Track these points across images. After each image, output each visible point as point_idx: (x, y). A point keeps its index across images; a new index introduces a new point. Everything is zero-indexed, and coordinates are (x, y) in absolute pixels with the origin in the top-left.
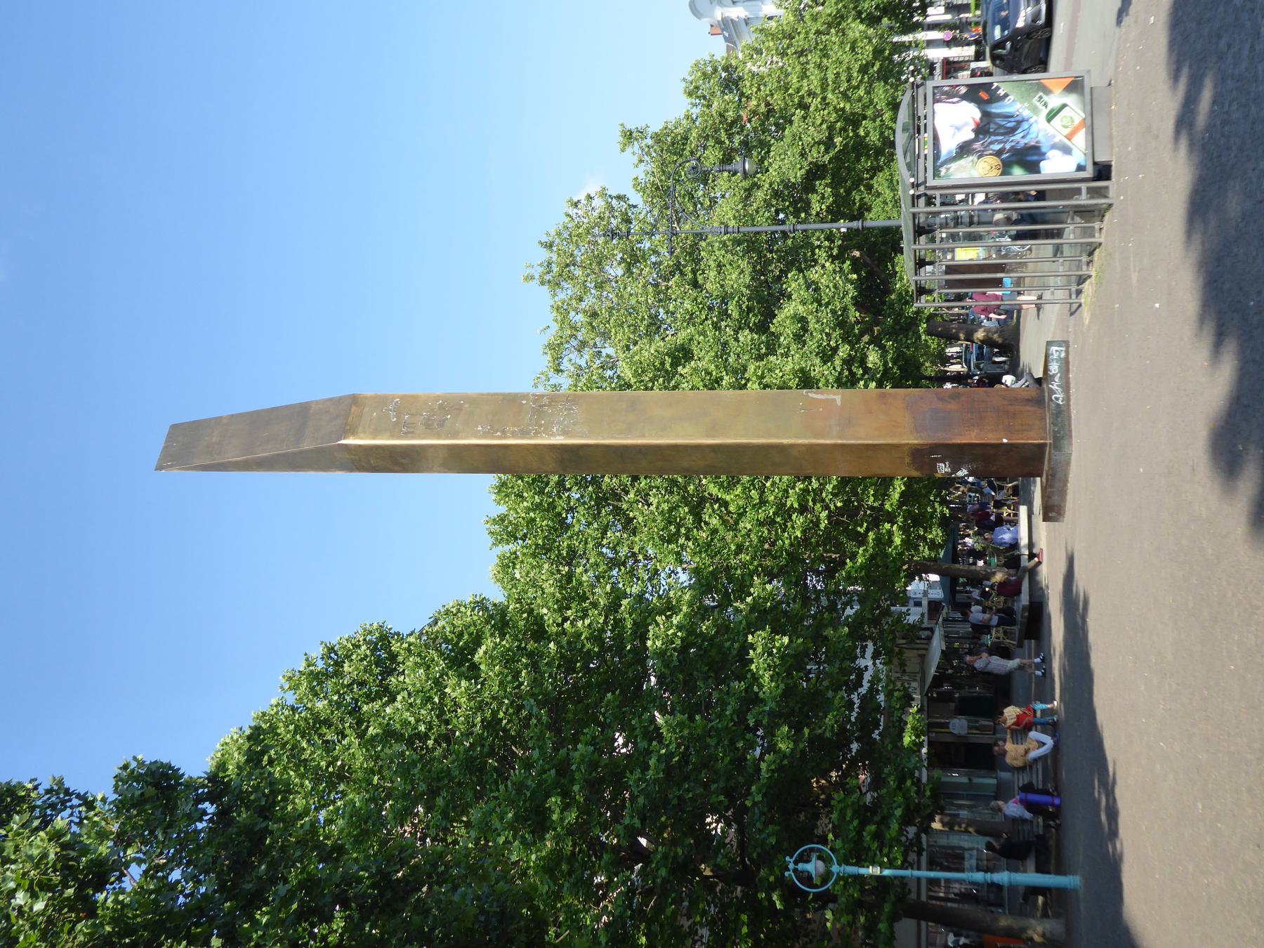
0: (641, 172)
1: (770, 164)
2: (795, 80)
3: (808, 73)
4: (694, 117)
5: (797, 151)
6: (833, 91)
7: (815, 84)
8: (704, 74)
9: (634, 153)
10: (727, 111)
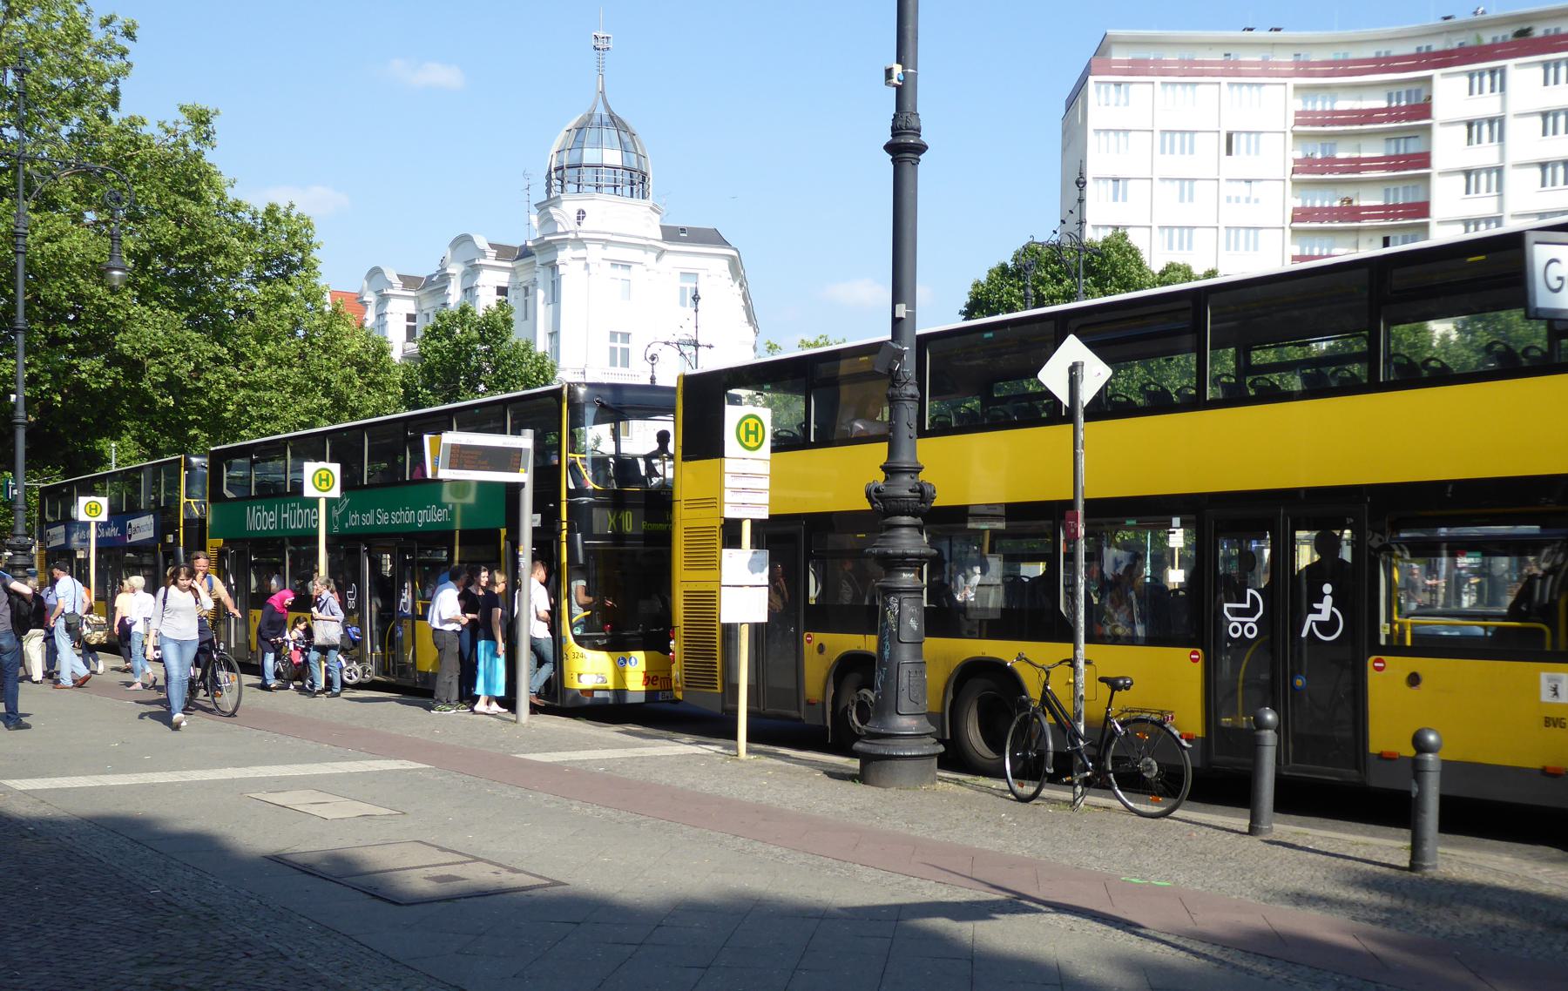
0: (150, 130)
1: (152, 309)
2: (267, 349)
3: (274, 367)
4: (240, 214)
5: (161, 345)
6: (249, 397)
7: (259, 375)
8: (295, 233)
9: (177, 123)
10: (227, 256)
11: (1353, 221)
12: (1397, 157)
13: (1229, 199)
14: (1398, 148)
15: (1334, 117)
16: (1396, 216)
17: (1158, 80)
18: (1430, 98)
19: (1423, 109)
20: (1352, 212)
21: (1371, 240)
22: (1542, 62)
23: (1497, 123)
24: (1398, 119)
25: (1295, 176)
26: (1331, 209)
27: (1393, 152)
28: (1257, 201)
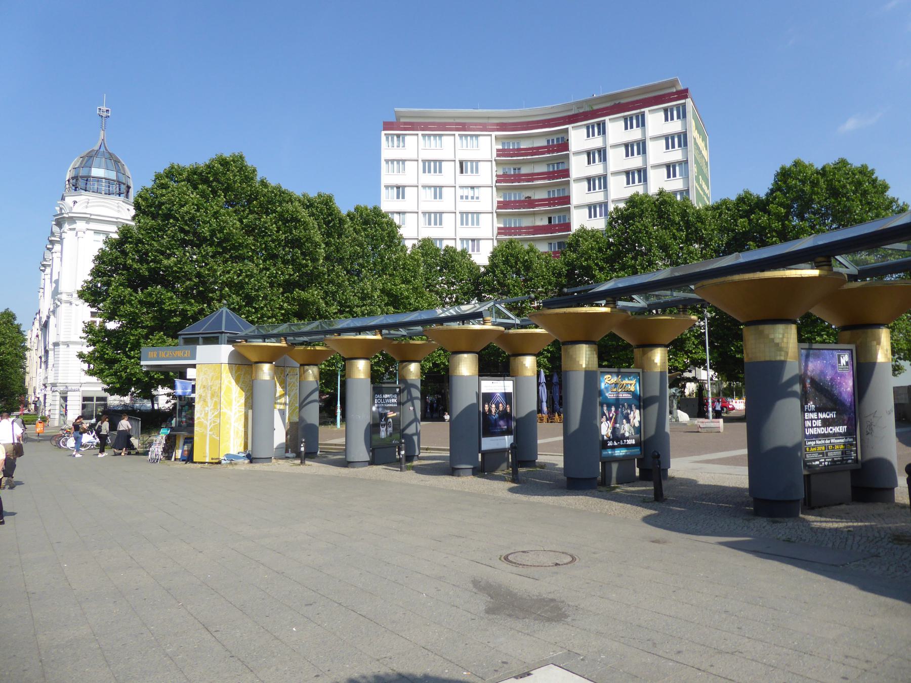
11: (530, 208)
12: (554, 172)
13: (462, 197)
14: (554, 169)
15: (519, 152)
16: (554, 205)
17: (420, 133)
18: (568, 140)
19: (565, 146)
20: (530, 203)
21: (542, 219)
22: (623, 117)
23: (602, 153)
24: (553, 152)
25: (497, 184)
26: (520, 202)
27: (551, 170)
28: (478, 198)
